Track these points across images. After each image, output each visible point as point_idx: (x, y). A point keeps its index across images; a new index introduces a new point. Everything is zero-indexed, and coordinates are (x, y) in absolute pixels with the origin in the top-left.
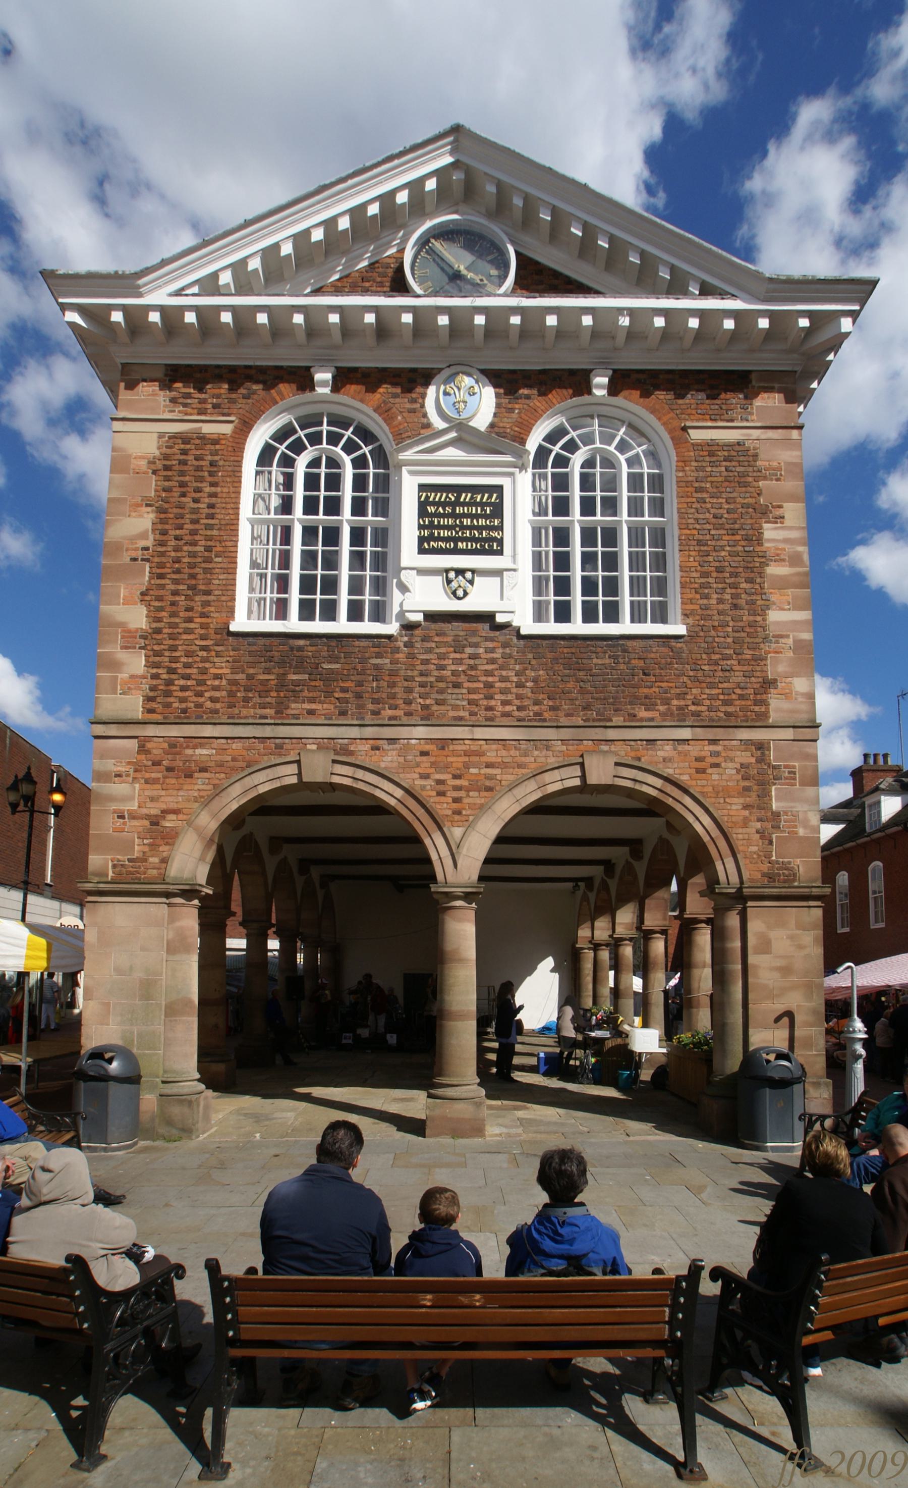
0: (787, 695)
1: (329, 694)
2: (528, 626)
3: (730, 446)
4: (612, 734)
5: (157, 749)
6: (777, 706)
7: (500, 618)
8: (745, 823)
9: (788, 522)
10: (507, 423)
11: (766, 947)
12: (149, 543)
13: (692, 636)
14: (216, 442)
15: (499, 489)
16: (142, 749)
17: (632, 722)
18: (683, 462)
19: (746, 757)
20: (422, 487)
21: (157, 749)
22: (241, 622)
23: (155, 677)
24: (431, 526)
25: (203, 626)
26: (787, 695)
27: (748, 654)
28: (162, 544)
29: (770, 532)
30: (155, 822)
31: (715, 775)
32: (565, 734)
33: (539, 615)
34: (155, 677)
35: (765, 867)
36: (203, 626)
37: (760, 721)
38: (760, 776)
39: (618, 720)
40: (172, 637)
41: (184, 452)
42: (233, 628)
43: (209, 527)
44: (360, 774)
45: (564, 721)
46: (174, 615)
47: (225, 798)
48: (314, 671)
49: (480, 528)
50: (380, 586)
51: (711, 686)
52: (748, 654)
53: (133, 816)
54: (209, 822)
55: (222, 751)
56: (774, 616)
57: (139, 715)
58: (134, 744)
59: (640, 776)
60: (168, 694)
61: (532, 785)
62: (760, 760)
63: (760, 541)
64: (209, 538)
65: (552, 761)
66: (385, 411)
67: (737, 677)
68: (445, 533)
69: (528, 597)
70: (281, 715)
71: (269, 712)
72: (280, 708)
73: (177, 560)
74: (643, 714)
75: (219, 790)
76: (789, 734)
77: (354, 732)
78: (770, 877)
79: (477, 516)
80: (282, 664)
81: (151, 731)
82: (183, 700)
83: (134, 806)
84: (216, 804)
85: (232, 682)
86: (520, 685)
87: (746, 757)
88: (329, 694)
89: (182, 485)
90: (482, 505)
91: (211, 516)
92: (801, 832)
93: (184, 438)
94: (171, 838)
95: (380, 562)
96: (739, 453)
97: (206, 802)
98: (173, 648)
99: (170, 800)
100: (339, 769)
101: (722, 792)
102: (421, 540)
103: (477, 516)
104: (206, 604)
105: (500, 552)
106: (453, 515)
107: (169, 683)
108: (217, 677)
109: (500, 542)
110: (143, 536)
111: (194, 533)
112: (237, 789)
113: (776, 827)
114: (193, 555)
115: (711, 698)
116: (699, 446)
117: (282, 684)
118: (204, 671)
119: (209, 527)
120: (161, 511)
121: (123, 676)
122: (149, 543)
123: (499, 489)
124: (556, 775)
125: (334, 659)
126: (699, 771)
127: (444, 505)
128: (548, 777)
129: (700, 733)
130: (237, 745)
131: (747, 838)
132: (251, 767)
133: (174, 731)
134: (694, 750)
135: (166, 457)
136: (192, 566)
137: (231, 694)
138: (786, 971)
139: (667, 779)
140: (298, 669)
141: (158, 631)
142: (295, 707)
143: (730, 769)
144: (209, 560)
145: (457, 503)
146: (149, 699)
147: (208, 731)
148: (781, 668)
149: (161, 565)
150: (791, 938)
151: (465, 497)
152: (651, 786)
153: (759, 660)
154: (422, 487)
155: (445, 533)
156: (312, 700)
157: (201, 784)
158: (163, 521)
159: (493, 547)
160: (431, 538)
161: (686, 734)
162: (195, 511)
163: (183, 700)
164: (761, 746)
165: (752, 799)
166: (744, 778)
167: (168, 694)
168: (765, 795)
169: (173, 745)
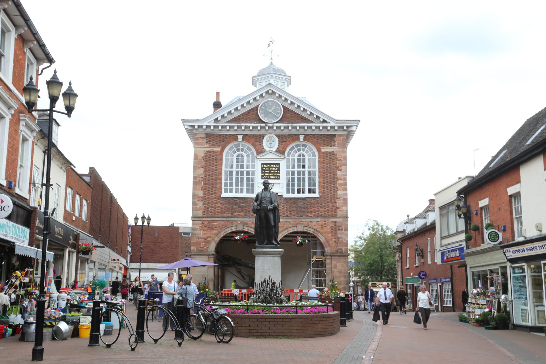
0: (342, 211)
1: (242, 211)
2: (286, 195)
3: (330, 153)
4: (303, 220)
5: (206, 223)
6: (339, 213)
7: (279, 194)
8: (332, 239)
9: (343, 171)
10: (281, 148)
11: (336, 267)
12: (203, 176)
13: (321, 197)
14: (217, 152)
15: (279, 164)
16: (203, 223)
17: (308, 217)
18: (320, 156)
19: (332, 225)
20: (262, 164)
21: (206, 223)
22: (224, 195)
23: (205, 207)
24: (264, 173)
25: (215, 195)
26: (342, 211)
27: (333, 201)
28: (206, 176)
29: (339, 173)
30: (205, 239)
31: (325, 229)
32: (293, 220)
33: (288, 192)
34: (205, 207)
35: (336, 249)
36: (215, 195)
37: (335, 216)
38: (335, 229)
39: (304, 216)
40: (208, 198)
41: (210, 155)
42: (222, 196)
43: (216, 173)
44: (249, 229)
45: (292, 217)
46: (209, 193)
47: (220, 234)
48: (239, 206)
49: (275, 173)
50: (253, 185)
51: (325, 209)
52: (333, 201)
53: (201, 238)
54: (217, 239)
55: (220, 223)
56: (339, 192)
57: (202, 215)
58: (201, 222)
59: (309, 229)
60: (208, 211)
61: (286, 231)
62: (335, 225)
63: (336, 175)
64: (216, 175)
65: (290, 226)
66: (254, 145)
67: (330, 207)
68: (267, 174)
69: (285, 188)
70: (232, 216)
71: (230, 215)
72: (232, 214)
73: (209, 180)
74: (310, 215)
75: (219, 232)
76: (341, 220)
77: (248, 219)
78: (337, 251)
79: (274, 170)
80: (232, 204)
81: (204, 219)
82: (211, 212)
83: (201, 236)
84: (219, 236)
85: (222, 208)
86: (283, 209)
87: (332, 225)
88: (242, 211)
89: (210, 163)
90: (275, 168)
91: (216, 170)
92: (344, 241)
93: (210, 152)
94: (209, 243)
95: (252, 180)
96: (333, 153)
97: (217, 235)
98: (209, 200)
99: (209, 235)
100: (245, 227)
101: (327, 233)
102: (262, 176)
103: (274, 170)
104: (216, 190)
105: (279, 179)
106: (269, 170)
107: (208, 208)
108: (218, 207)
109: (279, 176)
110: (201, 175)
111: (212, 174)
112: (223, 232)
113: (338, 240)
114: (212, 179)
115: (325, 211)
116: (323, 153)
117: (232, 209)
118: (215, 206)
119: (216, 173)
120: (205, 169)
121: (198, 207)
122: (203, 176)
123: (279, 164)
124: (291, 229)
125: (243, 203)
126: (322, 228)
127: (267, 168)
128: (289, 229)
129: (322, 219)
130: (223, 222)
131: (332, 242)
132: (226, 227)
133: (209, 219)
134: (321, 223)
135: (206, 156)
136: (212, 182)
137: (221, 211)
138: (340, 272)
139: (315, 229)
140: (236, 205)
141: (205, 197)
142: (235, 214)
143: (328, 227)
144: (216, 180)
145: (270, 167)
146: (204, 212)
147: (217, 219)
148: (340, 205)
149: (205, 182)
150: (342, 265)
151: (272, 166)
152: (311, 231)
153: (335, 202)
154: (262, 164)
155: (267, 174)
156: (239, 212)
157: (215, 231)
158: (205, 171)
159: (277, 178)
160: (264, 175)
161: (319, 220)
162: (213, 169)
163: (211, 212)
164: (335, 222)
165: (333, 234)
166: (332, 229)
167: (208, 211)
168: (336, 233)
169: (209, 222)
